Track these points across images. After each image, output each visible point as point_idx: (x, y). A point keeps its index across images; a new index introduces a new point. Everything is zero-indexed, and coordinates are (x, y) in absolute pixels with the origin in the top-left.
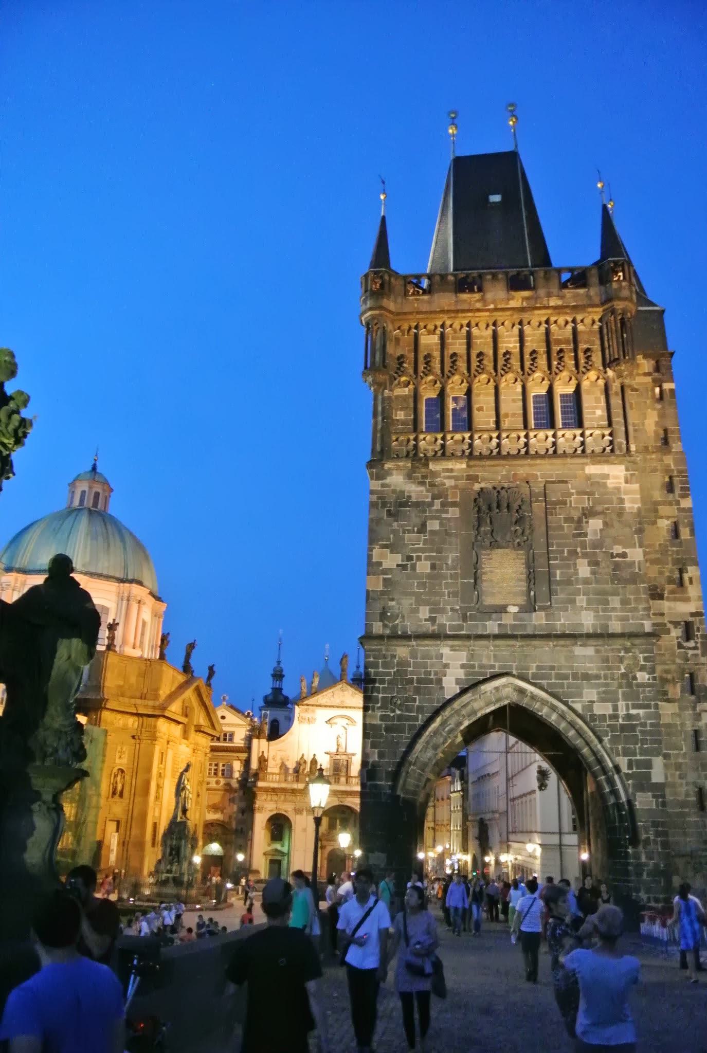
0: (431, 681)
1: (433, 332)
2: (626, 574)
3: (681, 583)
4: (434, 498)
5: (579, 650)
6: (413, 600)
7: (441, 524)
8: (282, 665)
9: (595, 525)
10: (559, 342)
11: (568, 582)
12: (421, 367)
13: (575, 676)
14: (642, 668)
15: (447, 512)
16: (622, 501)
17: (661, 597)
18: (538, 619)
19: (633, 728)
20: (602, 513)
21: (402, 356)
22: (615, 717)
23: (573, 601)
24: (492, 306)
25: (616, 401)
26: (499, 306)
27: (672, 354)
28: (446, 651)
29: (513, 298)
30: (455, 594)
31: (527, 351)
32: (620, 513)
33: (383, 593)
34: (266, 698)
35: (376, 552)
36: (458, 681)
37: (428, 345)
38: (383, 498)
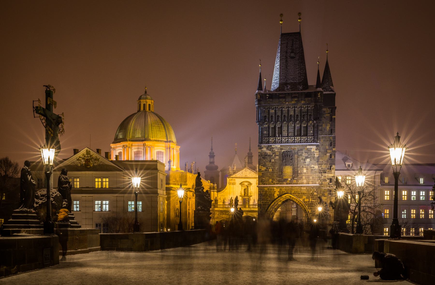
1: (273, 109)
3: (331, 169)
6: (268, 178)
8: (213, 151)
9: (308, 160)
10: (303, 112)
11: (302, 174)
12: (270, 119)
13: (301, 194)
14: (315, 192)
16: (314, 154)
17: (326, 173)
19: (312, 204)
21: (265, 116)
22: (309, 202)
23: (302, 178)
25: (316, 129)
30: (277, 176)
31: (296, 115)
32: (314, 157)
36: (277, 195)
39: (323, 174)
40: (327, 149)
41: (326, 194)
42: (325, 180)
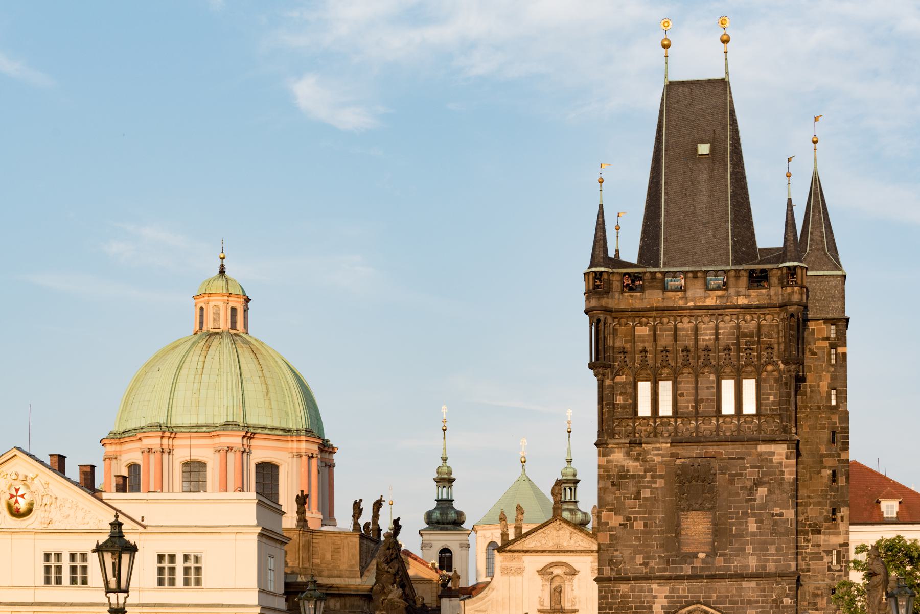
0: (644, 608)
2: (781, 529)
4: (645, 472)
5: (745, 584)
6: (631, 550)
7: (651, 492)
8: (448, 463)
9: (762, 491)
10: (745, 335)
13: (742, 602)
15: (656, 482)
16: (782, 473)
17: (819, 532)
18: (719, 562)
20: (769, 482)
23: (743, 549)
24: (691, 304)
26: (698, 304)
27: (848, 320)
28: (655, 586)
29: (709, 296)
30: (662, 546)
32: (781, 482)
33: (610, 545)
34: (429, 515)
35: (604, 514)
37: (640, 336)
38: (608, 471)
39: (810, 536)
40: (822, 456)
41: (822, 603)
42: (818, 557)
